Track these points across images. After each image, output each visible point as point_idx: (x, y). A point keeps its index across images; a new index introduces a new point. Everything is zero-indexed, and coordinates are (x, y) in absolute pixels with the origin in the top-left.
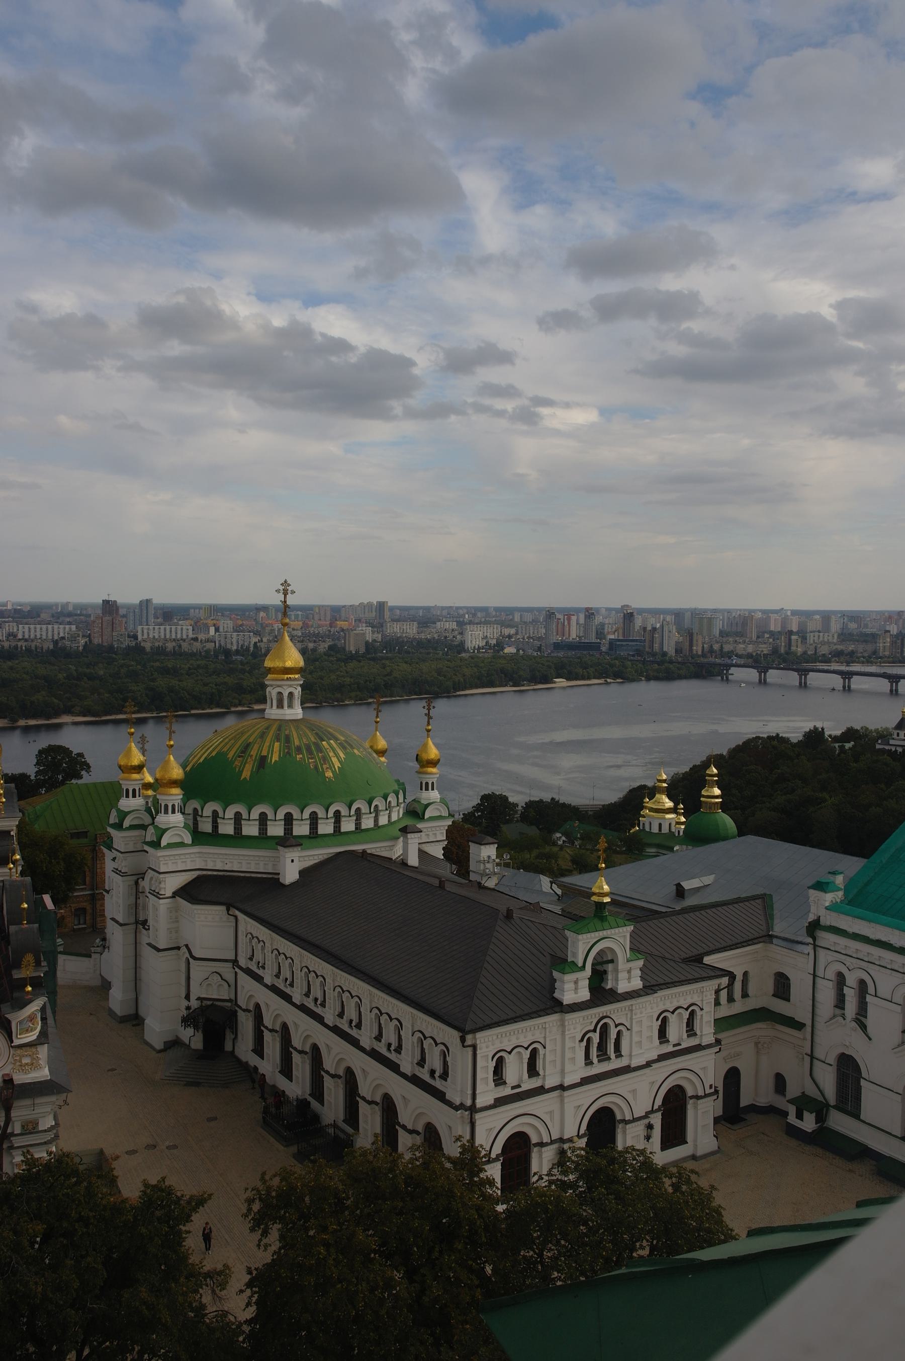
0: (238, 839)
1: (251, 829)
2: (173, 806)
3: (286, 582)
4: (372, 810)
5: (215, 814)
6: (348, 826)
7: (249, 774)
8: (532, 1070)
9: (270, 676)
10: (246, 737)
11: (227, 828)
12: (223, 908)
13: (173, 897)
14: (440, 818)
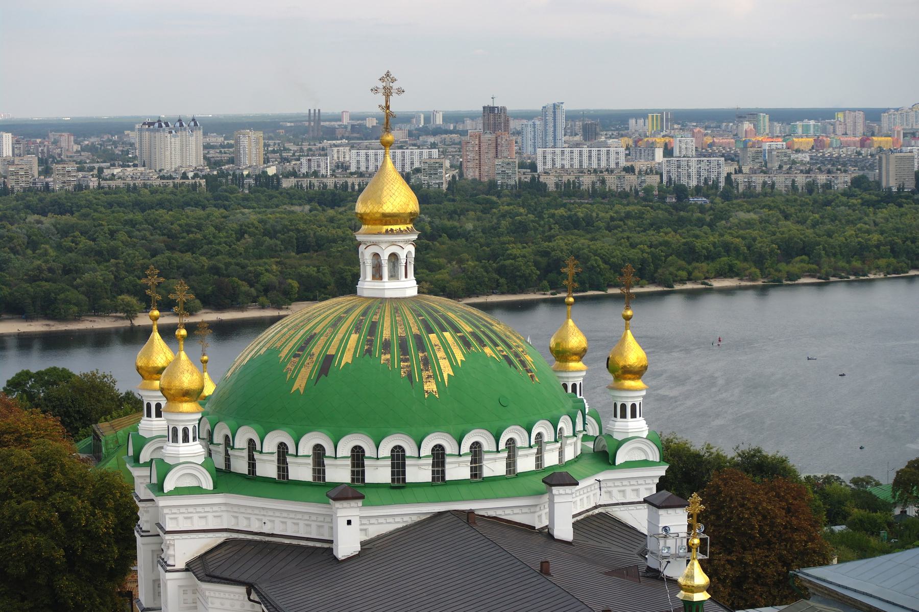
1: (301, 471)
2: (185, 431)
3: (388, 75)
4: (502, 445)
6: (458, 470)
7: (303, 385)
9: (364, 227)
10: (311, 325)
11: (268, 468)
12: (242, 590)
13: (186, 570)
14: (645, 463)
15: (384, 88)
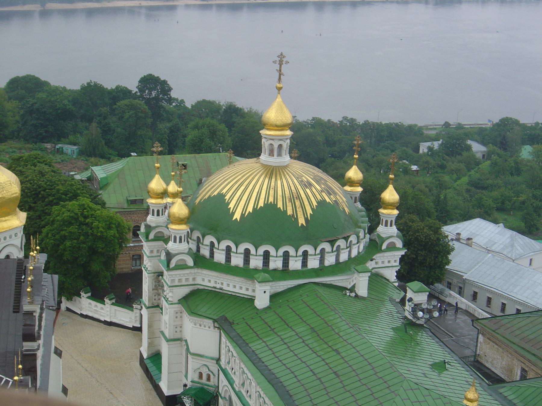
1: (237, 261)
3: (282, 54)
5: (212, 244)
6: (313, 263)
11: (220, 257)
13: (179, 303)
15: (279, 61)
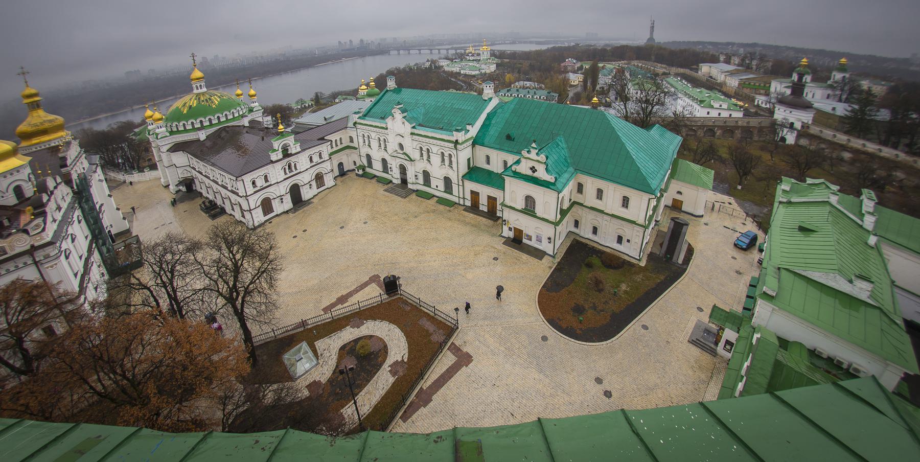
0: (186, 131)
1: (189, 127)
8: (267, 181)
